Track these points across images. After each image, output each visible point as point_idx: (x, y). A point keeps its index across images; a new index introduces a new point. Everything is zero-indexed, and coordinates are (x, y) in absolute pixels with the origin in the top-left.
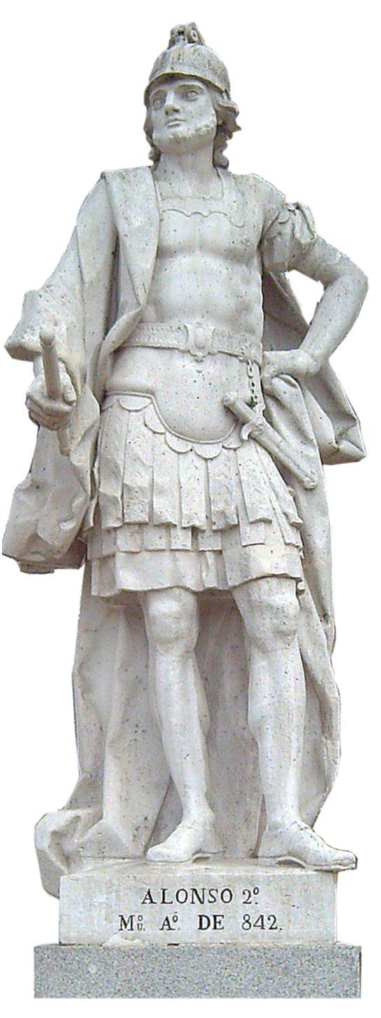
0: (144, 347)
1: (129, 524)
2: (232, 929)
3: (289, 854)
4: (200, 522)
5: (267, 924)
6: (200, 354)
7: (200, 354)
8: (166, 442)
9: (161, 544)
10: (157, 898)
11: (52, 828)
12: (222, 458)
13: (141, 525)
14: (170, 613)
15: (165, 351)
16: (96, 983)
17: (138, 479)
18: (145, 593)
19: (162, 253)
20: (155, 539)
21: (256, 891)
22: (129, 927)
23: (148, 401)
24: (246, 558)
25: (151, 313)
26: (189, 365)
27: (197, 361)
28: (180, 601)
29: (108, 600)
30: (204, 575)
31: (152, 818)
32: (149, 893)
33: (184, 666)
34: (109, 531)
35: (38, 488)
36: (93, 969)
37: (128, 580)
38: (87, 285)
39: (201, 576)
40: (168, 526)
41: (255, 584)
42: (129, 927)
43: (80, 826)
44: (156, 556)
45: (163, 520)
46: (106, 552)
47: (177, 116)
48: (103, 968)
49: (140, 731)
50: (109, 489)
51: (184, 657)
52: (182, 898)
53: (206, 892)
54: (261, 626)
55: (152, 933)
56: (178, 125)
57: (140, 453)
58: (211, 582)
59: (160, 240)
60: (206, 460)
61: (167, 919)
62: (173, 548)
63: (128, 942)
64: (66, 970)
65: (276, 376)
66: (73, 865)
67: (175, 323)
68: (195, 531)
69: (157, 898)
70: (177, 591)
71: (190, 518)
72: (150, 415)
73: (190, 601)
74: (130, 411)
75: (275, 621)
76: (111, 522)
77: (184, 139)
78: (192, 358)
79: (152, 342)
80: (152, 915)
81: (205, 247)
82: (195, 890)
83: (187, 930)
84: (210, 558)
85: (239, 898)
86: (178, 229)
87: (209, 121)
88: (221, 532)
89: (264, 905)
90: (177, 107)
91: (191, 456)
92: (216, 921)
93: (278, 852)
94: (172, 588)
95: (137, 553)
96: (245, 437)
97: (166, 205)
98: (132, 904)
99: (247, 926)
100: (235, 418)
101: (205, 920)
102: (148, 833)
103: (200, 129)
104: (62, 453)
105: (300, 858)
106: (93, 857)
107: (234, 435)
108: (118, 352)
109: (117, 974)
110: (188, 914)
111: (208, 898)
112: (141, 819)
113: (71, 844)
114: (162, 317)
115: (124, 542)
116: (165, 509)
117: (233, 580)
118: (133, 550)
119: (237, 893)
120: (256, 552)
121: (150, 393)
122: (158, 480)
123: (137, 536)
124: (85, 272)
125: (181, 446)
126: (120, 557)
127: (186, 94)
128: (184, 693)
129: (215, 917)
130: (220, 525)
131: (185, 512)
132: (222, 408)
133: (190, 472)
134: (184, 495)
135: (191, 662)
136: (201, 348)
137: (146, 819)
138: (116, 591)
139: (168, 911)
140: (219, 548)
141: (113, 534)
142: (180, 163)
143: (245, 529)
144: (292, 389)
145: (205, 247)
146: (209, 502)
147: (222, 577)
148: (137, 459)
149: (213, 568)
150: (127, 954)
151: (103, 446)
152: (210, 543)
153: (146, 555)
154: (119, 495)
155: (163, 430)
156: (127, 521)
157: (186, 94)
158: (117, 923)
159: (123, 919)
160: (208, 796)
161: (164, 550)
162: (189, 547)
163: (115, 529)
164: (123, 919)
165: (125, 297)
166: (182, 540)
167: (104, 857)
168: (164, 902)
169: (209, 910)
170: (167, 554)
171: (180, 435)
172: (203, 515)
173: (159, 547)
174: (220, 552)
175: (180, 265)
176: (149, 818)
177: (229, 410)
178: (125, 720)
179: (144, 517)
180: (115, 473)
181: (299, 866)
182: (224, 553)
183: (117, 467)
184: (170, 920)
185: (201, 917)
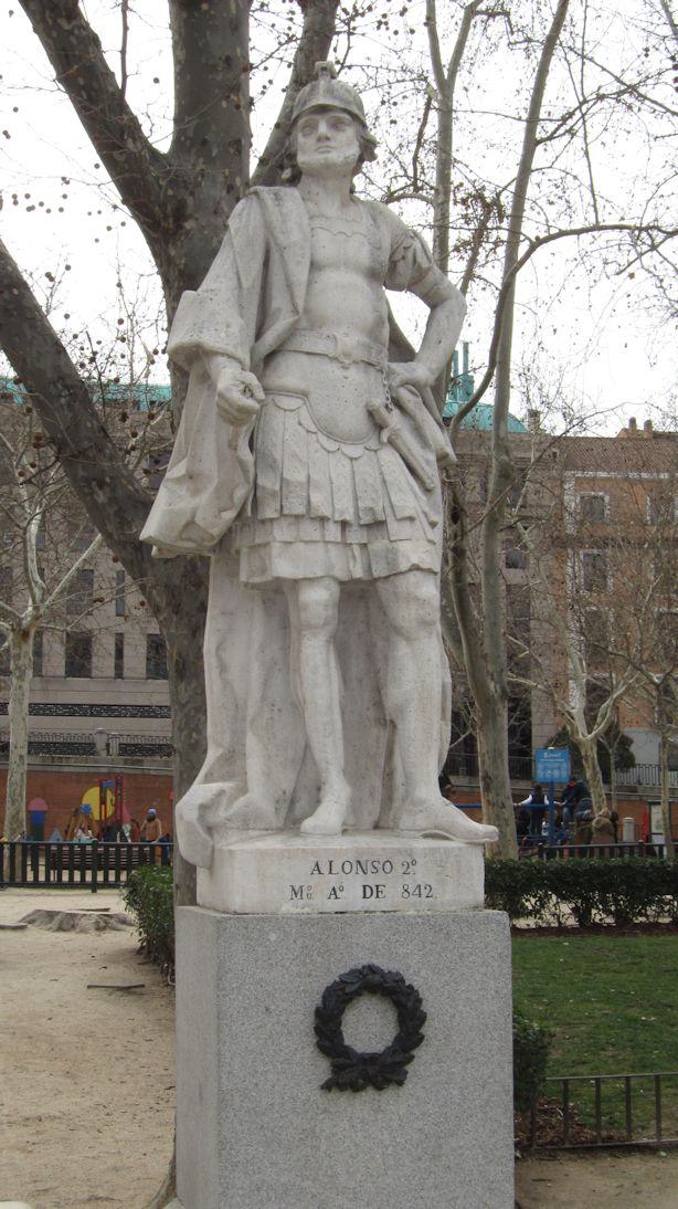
0: (295, 351)
1: (285, 516)
2: (392, 897)
3: (436, 828)
4: (349, 517)
5: (424, 892)
6: (347, 361)
7: (347, 361)
8: (318, 441)
9: (316, 535)
11: (200, 801)
12: (365, 458)
13: (297, 517)
14: (318, 599)
15: (233, 361)
16: (276, 950)
17: (295, 474)
18: (296, 581)
19: (314, 266)
20: (310, 530)
21: (414, 862)
22: (299, 896)
23: (301, 402)
24: (395, 552)
25: (304, 323)
26: (339, 373)
27: (343, 367)
28: (329, 590)
29: (254, 586)
30: (351, 565)
31: (289, 790)
32: (317, 865)
33: (328, 651)
34: (263, 522)
35: (191, 478)
36: (273, 937)
37: (283, 568)
38: (245, 292)
39: (348, 567)
40: (323, 519)
41: (402, 577)
42: (299, 896)
43: (224, 800)
44: (312, 546)
45: (320, 513)
46: (257, 541)
47: (328, 143)
48: (282, 936)
49: (276, 711)
50: (268, 482)
51: (328, 642)
52: (347, 870)
53: (369, 864)
54: (405, 615)
56: (329, 152)
57: (297, 450)
58: (358, 573)
59: (312, 255)
60: (351, 459)
61: (334, 889)
62: (327, 539)
63: (299, 910)
64: (248, 938)
65: (402, 386)
66: (216, 836)
67: (325, 331)
68: (344, 524)
69: (324, 869)
70: (327, 581)
71: (342, 513)
72: (304, 412)
73: (335, 589)
74: (285, 410)
75: (421, 612)
76: (269, 512)
77: (335, 165)
78: (340, 365)
79: (306, 347)
81: (347, 264)
82: (359, 862)
83: (352, 898)
84: (356, 550)
85: (399, 869)
86: (327, 247)
87: (354, 151)
88: (368, 526)
89: (421, 875)
90: (329, 135)
91: (338, 455)
93: (424, 825)
94: (322, 577)
95: (291, 543)
96: (385, 439)
97: (316, 223)
98: (300, 873)
99: (406, 894)
100: (378, 426)
101: (368, 890)
102: (286, 805)
103: (348, 157)
104: (230, 446)
105: (447, 831)
106: (238, 828)
107: (375, 437)
108: (270, 357)
109: (295, 941)
110: (353, 887)
111: (370, 868)
112: (281, 793)
113: (221, 814)
114: (312, 327)
115: (281, 532)
116: (319, 500)
117: (379, 570)
118: (289, 540)
120: (403, 547)
121: (304, 395)
122: (313, 476)
123: (293, 527)
124: (243, 279)
125: (332, 446)
126: (276, 548)
127: (336, 125)
129: (377, 886)
130: (366, 519)
131: (337, 507)
132: (367, 414)
133: (339, 470)
134: (335, 490)
135: (332, 648)
136: (346, 355)
137: (284, 792)
138: (270, 578)
139: (333, 881)
140: (365, 542)
141: (269, 524)
142: (324, 186)
143: (393, 526)
144: (415, 398)
145: (347, 264)
146: (356, 499)
148: (294, 455)
149: (359, 560)
150: (304, 922)
151: (259, 441)
152: (356, 536)
153: (301, 546)
154: (277, 488)
155: (315, 430)
156: (286, 512)
157: (336, 125)
158: (288, 891)
159: (293, 889)
160: (345, 772)
161: (318, 542)
162: (339, 540)
163: (272, 520)
164: (293, 889)
165: (279, 301)
166: (333, 532)
167: (248, 829)
168: (330, 873)
169: (372, 880)
170: (321, 545)
171: (330, 435)
172: (352, 510)
173: (314, 539)
174: (365, 545)
175: (330, 278)
176: (287, 792)
178: (263, 699)
179: (301, 510)
180: (273, 466)
181: (447, 839)
182: (369, 546)
183: (275, 461)
184: (337, 890)
185: (364, 887)
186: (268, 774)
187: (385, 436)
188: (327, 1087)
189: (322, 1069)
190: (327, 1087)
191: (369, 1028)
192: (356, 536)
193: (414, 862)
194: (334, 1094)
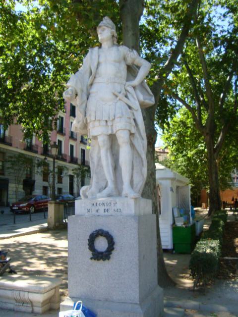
2: (111, 212)
4: (107, 119)
10: (95, 205)
14: (102, 140)
20: (97, 123)
21: (116, 203)
33: (107, 152)
51: (107, 150)
55: (94, 212)
58: (110, 132)
68: (106, 121)
69: (95, 205)
73: (106, 138)
76: (88, 121)
80: (94, 209)
89: (118, 206)
92: (107, 210)
98: (89, 207)
119: (112, 204)
128: (107, 156)
130: (111, 119)
135: (109, 151)
139: (97, 208)
147: (112, 131)
158: (87, 211)
166: (104, 123)
169: (106, 208)
177: (114, 94)
186: (97, 183)
187: (118, 99)
188: (91, 258)
189: (89, 254)
190: (91, 258)
191: (101, 244)
192: (109, 123)
193: (116, 203)
194: (93, 260)
